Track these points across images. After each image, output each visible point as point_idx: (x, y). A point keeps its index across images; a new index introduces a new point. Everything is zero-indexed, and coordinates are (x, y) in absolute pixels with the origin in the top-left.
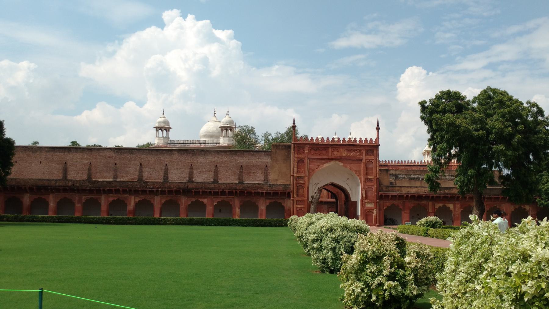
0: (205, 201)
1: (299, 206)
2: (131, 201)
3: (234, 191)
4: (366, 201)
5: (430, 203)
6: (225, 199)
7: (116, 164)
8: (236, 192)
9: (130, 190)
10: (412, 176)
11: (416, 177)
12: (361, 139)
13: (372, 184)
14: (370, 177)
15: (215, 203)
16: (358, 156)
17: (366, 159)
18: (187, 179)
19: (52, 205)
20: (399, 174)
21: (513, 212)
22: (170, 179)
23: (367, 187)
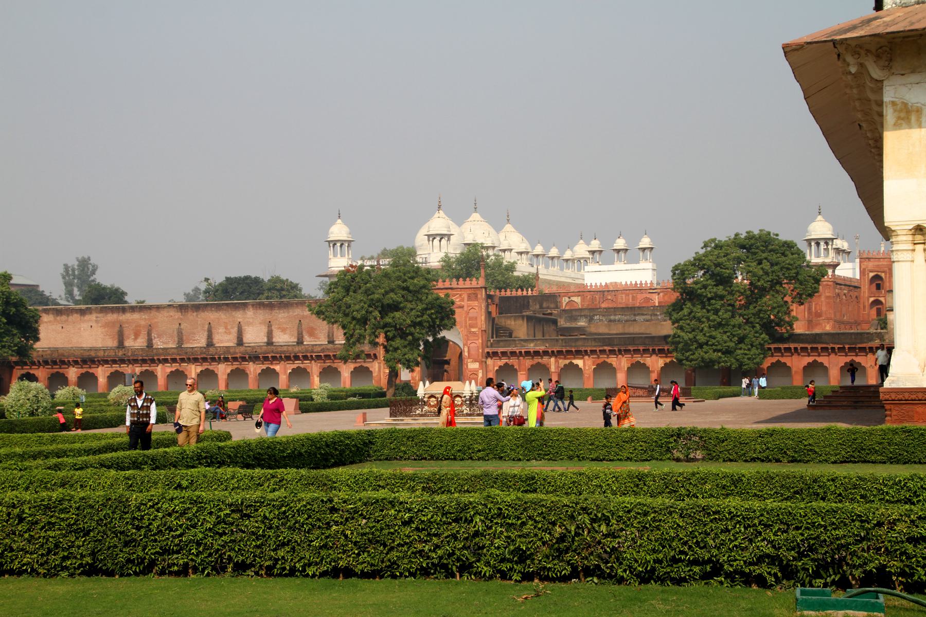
0: (277, 368)
2: (191, 372)
5: (553, 359)
6: (301, 366)
10: (612, 317)
11: (617, 318)
14: (473, 330)
18: (266, 340)
19: (102, 380)
22: (245, 340)
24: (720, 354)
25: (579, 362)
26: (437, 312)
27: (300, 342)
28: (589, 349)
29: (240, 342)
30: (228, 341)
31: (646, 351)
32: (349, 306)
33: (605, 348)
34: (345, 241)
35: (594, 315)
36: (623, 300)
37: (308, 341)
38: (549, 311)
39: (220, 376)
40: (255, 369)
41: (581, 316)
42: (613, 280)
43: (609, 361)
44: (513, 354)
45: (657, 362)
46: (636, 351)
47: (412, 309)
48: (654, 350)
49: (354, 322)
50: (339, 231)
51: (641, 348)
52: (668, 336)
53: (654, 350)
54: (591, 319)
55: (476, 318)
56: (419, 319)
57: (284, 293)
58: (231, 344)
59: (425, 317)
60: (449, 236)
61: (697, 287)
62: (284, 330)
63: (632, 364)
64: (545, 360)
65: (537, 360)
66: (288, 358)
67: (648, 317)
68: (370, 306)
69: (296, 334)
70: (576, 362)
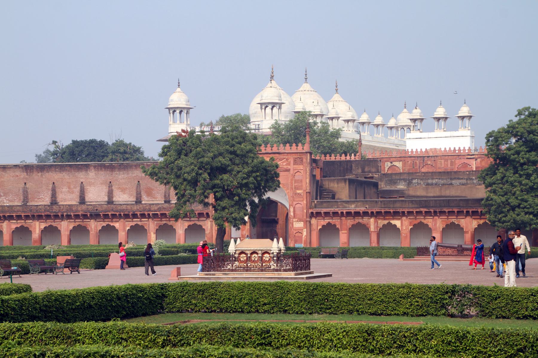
0: (117, 225)
2: (35, 228)
3: (146, 213)
4: (294, 220)
5: (372, 220)
6: (139, 223)
7: (25, 183)
8: (149, 214)
9: (33, 216)
10: (430, 181)
13: (302, 199)
14: (298, 192)
16: (285, 167)
17: (294, 170)
18: (106, 199)
21: (475, 229)
22: (87, 199)
23: (295, 203)
24: (531, 216)
25: (397, 223)
26: (262, 174)
27: (138, 201)
28: (406, 210)
29: (82, 201)
30: (71, 200)
31: (460, 213)
32: (180, 169)
33: (422, 209)
34: (184, 108)
35: (412, 179)
36: (442, 165)
37: (146, 200)
38: (370, 175)
39: (62, 233)
40: (96, 226)
41: (400, 180)
42: (433, 147)
43: (425, 222)
44: (335, 214)
45: (471, 224)
46: (451, 213)
47: (238, 172)
48: (468, 212)
49: (185, 183)
50: (178, 99)
51: (456, 210)
52: (482, 199)
53: (468, 212)
54: (409, 183)
55: (301, 181)
56: (245, 181)
57: (127, 156)
58: (74, 203)
59: (251, 179)
60: (280, 104)
61: (509, 153)
62: (123, 190)
63: (447, 225)
64: (365, 220)
65: (359, 220)
66: (126, 216)
67: (464, 181)
68: (200, 168)
69: (135, 194)
70: (394, 222)
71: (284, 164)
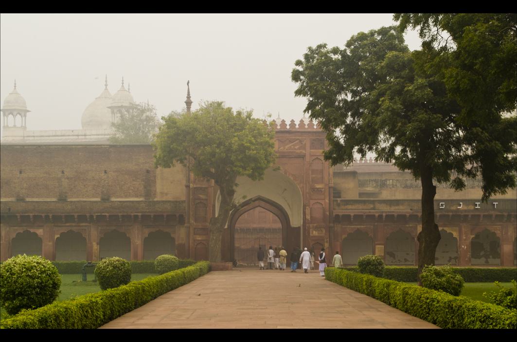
0: (40, 232)
1: (199, 238)
3: (88, 215)
6: (74, 229)
12: (293, 121)
14: (318, 186)
15: (57, 236)
16: (298, 151)
20: (386, 180)
35: (386, 180)
44: (371, 217)
71: (297, 147)
